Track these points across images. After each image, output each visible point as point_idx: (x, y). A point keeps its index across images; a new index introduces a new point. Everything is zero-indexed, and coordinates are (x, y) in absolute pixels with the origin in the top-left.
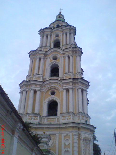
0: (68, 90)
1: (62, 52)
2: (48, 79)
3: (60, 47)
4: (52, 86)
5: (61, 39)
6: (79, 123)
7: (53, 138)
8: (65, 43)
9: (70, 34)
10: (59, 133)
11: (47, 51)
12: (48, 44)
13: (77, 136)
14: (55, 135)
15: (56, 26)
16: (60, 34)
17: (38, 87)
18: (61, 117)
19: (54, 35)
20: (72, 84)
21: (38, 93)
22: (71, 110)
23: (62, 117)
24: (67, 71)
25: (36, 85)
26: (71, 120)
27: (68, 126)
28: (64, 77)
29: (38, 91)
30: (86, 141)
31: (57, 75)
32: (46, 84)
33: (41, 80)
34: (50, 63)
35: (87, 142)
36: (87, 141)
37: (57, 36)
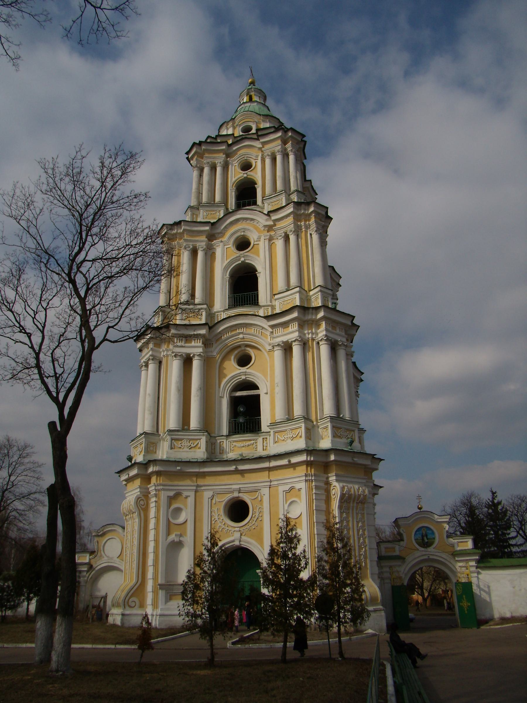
0: (287, 348)
1: (262, 220)
2: (224, 316)
3: (255, 203)
4: (241, 336)
6: (327, 452)
7: (254, 498)
10: (269, 484)
11: (212, 221)
13: (323, 492)
14: (256, 491)
15: (238, 132)
17: (193, 344)
18: (272, 431)
20: (301, 326)
23: (275, 432)
25: (188, 338)
26: (301, 444)
27: (295, 460)
28: (275, 305)
30: (351, 505)
31: (254, 301)
32: (220, 333)
33: (203, 321)
34: (228, 260)
35: (353, 507)
36: (354, 501)
37: (246, 166)
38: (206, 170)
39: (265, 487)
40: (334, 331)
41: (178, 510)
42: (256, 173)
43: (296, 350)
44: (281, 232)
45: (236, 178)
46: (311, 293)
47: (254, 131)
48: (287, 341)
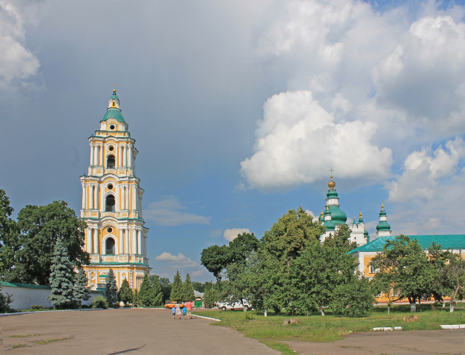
0: (124, 231)
1: (118, 179)
4: (109, 223)
5: (116, 155)
8: (120, 164)
9: (127, 148)
12: (101, 164)
16: (114, 147)
18: (119, 256)
19: (108, 147)
20: (128, 225)
21: (96, 232)
22: (126, 252)
24: (123, 208)
25: (93, 223)
29: (96, 230)
33: (97, 217)
38: (96, 149)
39: (116, 272)
40: (137, 226)
41: (93, 277)
42: (115, 153)
43: (126, 231)
44: (123, 186)
45: (108, 154)
46: (132, 211)
47: (115, 130)
48: (123, 229)
